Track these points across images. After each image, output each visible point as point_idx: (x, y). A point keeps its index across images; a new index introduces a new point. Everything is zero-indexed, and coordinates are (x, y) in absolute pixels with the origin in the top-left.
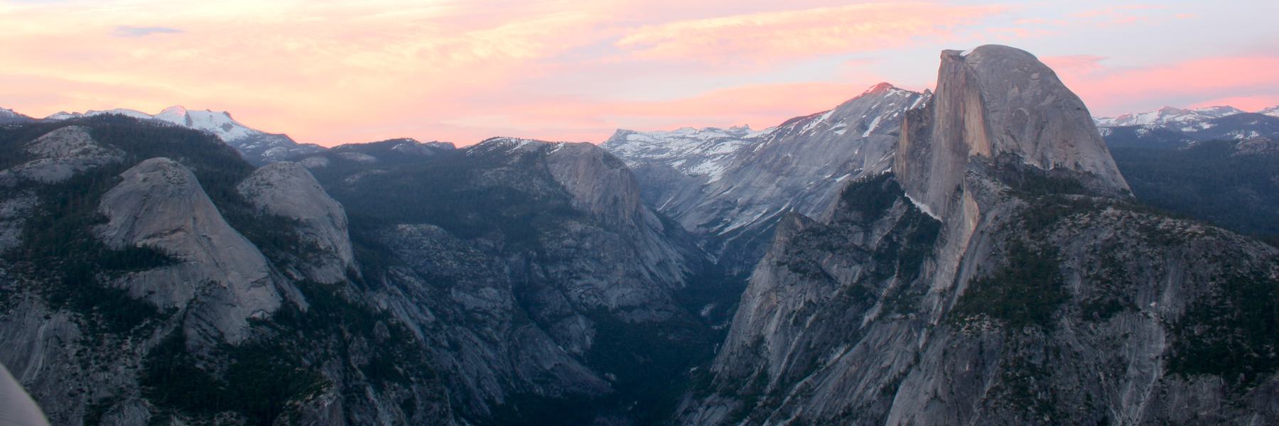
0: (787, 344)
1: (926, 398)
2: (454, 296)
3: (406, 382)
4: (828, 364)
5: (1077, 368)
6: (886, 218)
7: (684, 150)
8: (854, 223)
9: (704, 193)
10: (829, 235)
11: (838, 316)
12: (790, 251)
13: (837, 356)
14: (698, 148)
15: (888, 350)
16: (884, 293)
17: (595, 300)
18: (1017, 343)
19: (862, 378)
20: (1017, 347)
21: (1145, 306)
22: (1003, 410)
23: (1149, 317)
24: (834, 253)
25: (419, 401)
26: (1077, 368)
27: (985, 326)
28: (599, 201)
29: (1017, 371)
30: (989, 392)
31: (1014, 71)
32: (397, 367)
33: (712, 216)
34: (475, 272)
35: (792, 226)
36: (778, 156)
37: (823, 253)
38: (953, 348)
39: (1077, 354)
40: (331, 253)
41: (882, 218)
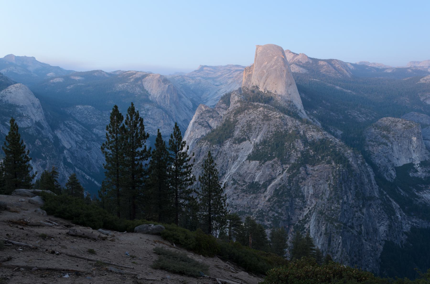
2: (94, 131)
3: (45, 159)
7: (223, 74)
8: (223, 108)
9: (217, 93)
12: (199, 118)
14: (227, 73)
17: (152, 133)
21: (252, 140)
23: (251, 143)
24: (213, 119)
25: (48, 165)
27: (205, 144)
28: (159, 96)
30: (198, 164)
32: (42, 154)
34: (104, 123)
39: (226, 153)
40: (28, 117)
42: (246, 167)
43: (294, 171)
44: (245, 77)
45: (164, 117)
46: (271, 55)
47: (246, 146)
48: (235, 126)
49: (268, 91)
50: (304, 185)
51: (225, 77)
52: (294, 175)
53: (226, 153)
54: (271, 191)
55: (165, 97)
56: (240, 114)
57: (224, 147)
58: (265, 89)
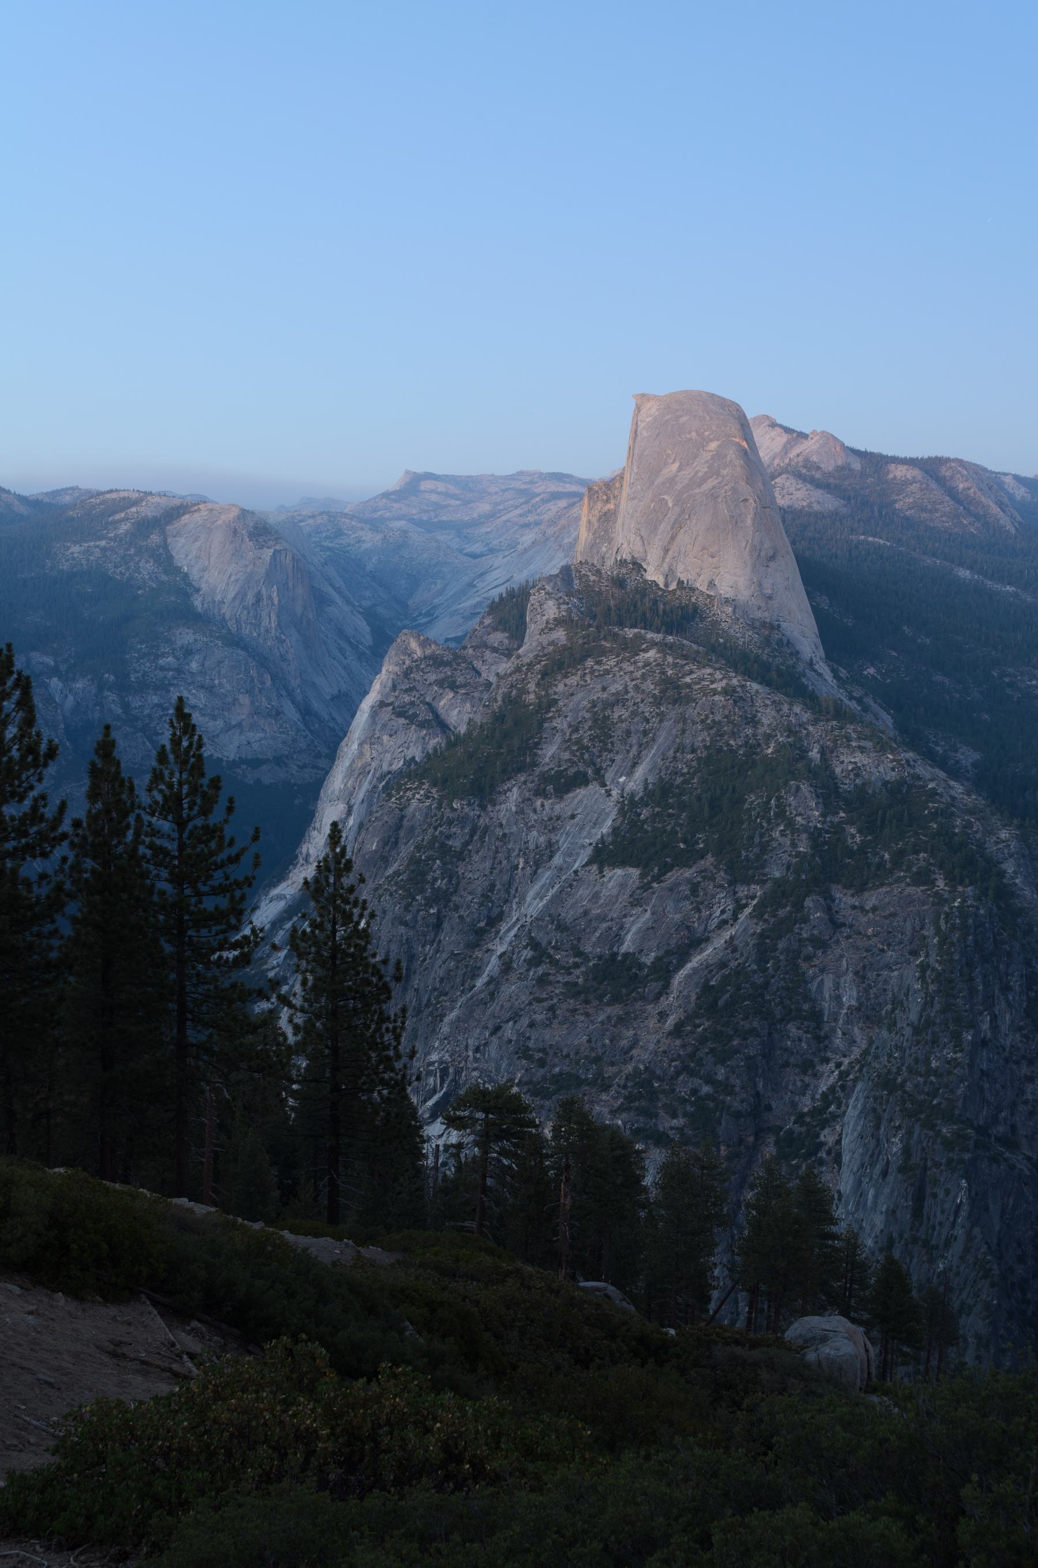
7: (499, 511)
8: (495, 650)
9: (475, 586)
12: (399, 687)
14: (516, 507)
21: (612, 782)
23: (609, 795)
27: (418, 796)
28: (235, 598)
30: (388, 877)
37: (441, 691)
39: (505, 835)
42: (588, 891)
43: (782, 913)
44: (589, 522)
45: (252, 681)
46: (694, 435)
48: (546, 725)
49: (680, 583)
50: (823, 970)
51: (508, 521)
53: (505, 835)
54: (685, 993)
55: (258, 598)
56: (566, 676)
57: (498, 807)
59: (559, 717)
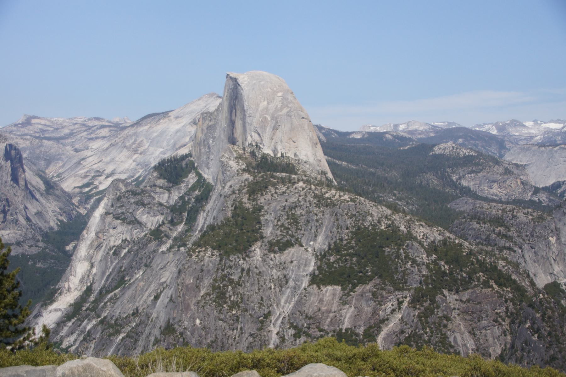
0: (107, 268)
1: (168, 300)
4: (132, 281)
5: (259, 281)
6: (183, 185)
7: (75, 133)
8: (161, 187)
9: (82, 164)
10: (143, 195)
11: (142, 249)
12: (115, 206)
13: (137, 276)
14: (85, 131)
15: (165, 271)
16: (175, 234)
18: (225, 266)
19: (147, 290)
20: (224, 268)
21: (306, 244)
22: (208, 307)
23: (307, 251)
24: (145, 208)
26: (259, 281)
27: (207, 255)
29: (221, 283)
30: (202, 296)
31: (267, 90)
33: (86, 181)
35: (118, 189)
36: (135, 140)
37: (137, 207)
38: (185, 268)
39: (260, 272)
41: (180, 184)
44: (202, 130)
46: (269, 90)
47: (297, 257)
51: (82, 137)
52: (428, 313)
53: (260, 272)
56: (262, 195)
57: (252, 259)
58: (275, 151)
59: (267, 214)
